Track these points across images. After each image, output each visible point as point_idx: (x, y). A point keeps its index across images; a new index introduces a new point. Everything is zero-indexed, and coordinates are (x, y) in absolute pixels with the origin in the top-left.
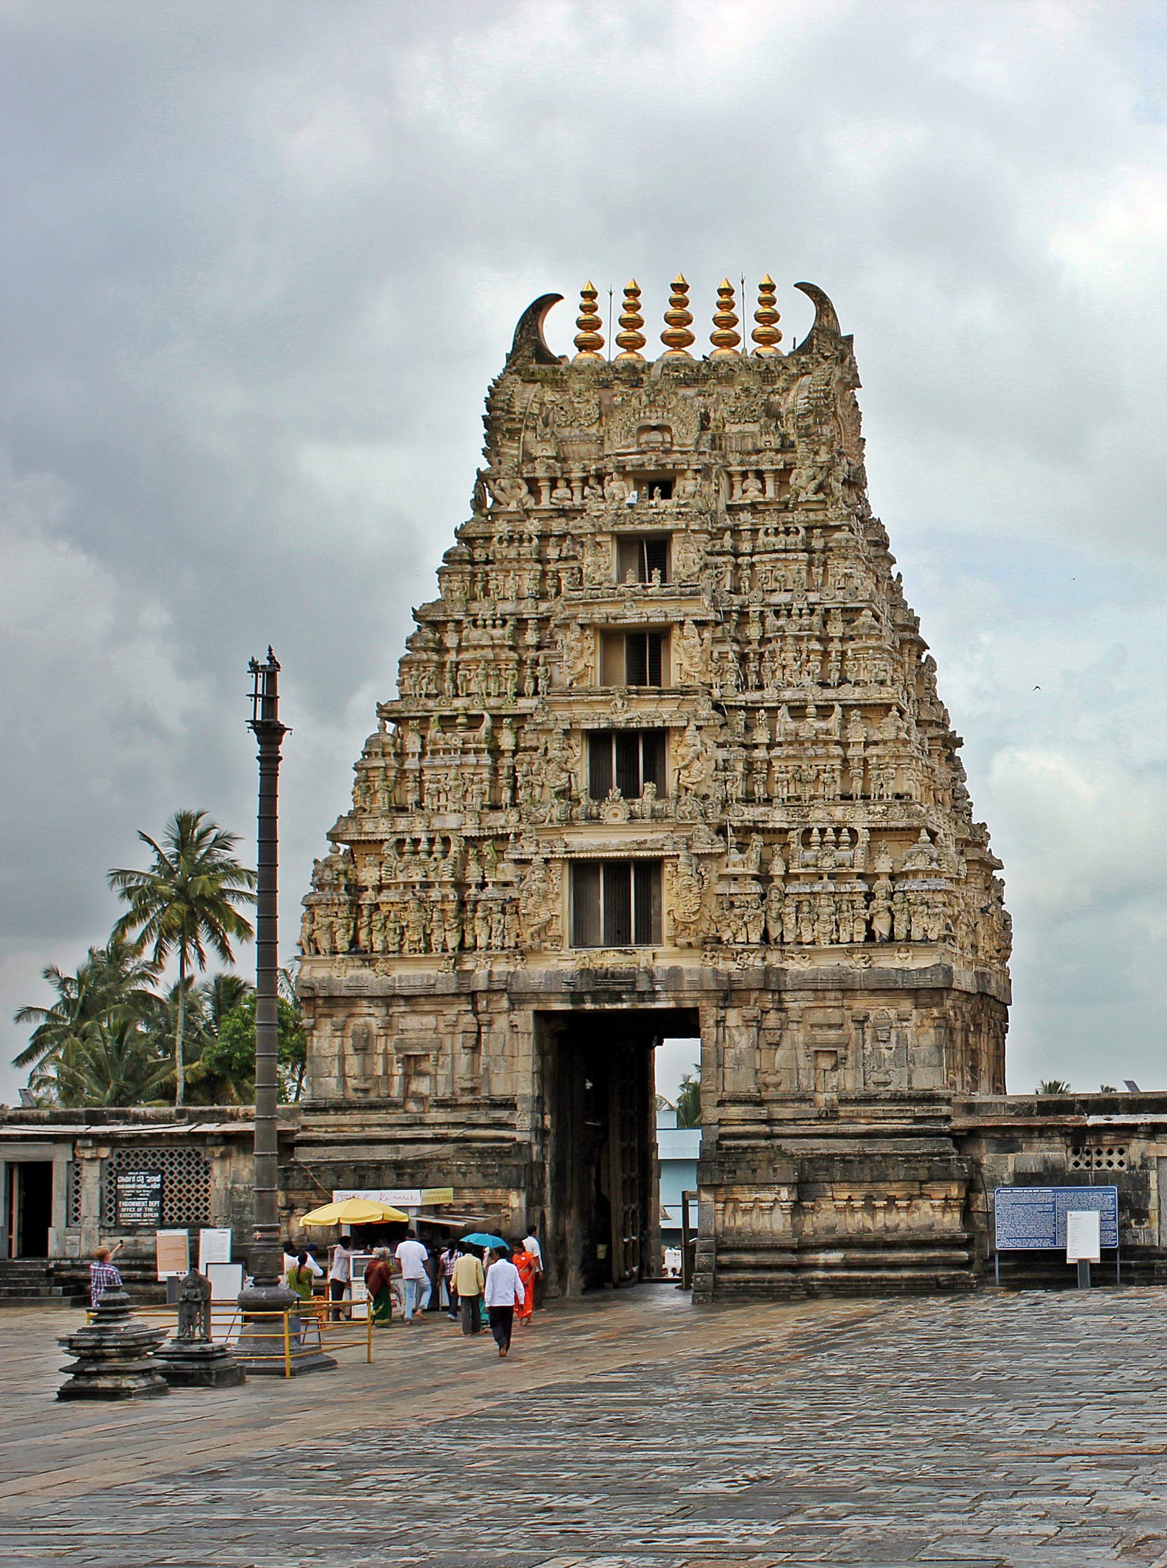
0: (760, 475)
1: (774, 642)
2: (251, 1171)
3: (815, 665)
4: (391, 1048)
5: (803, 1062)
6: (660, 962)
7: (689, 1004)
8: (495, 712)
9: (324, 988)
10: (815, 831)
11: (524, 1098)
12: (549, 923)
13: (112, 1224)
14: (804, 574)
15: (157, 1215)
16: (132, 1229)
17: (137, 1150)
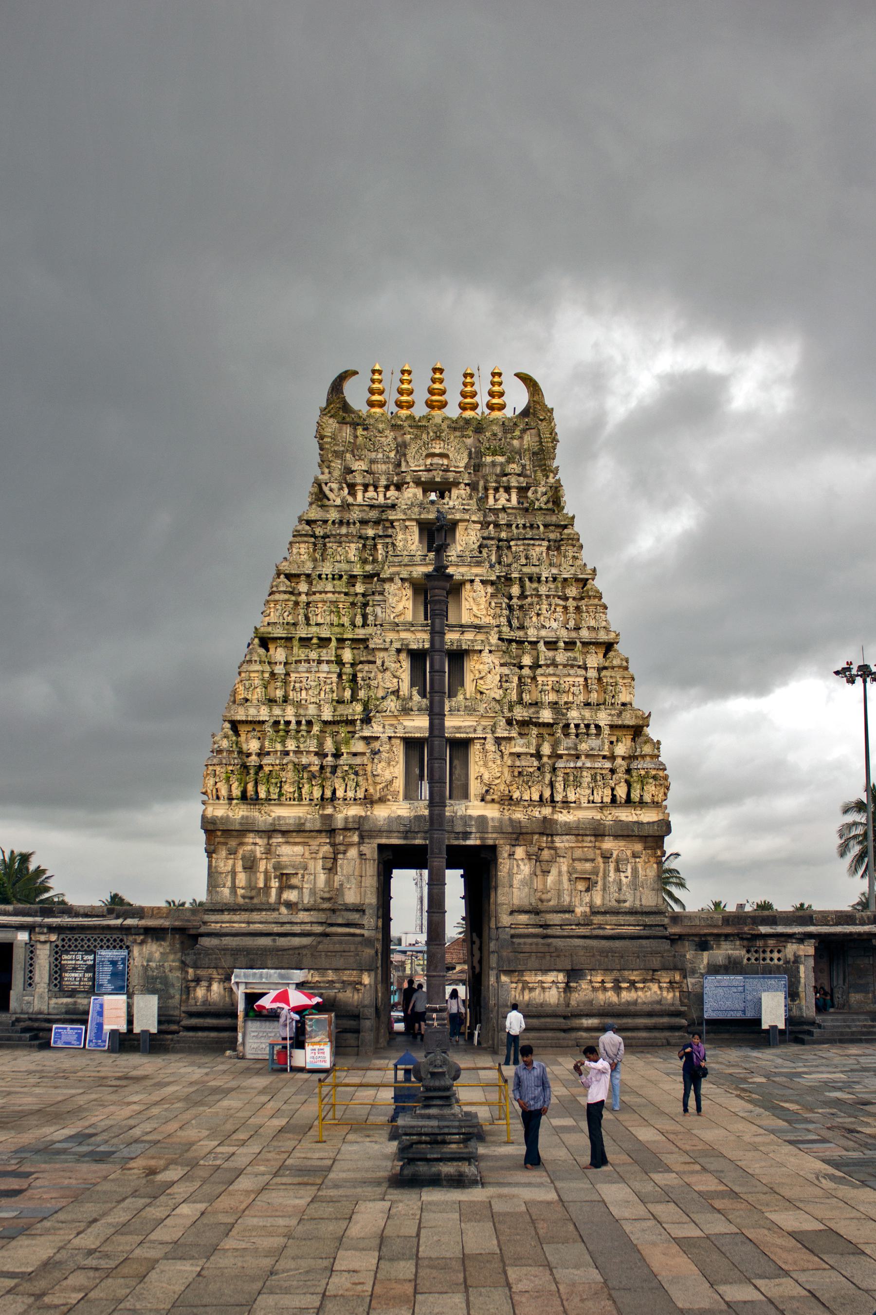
0: (507, 489)
1: (529, 598)
2: (161, 953)
3: (559, 615)
4: (270, 867)
5: (566, 884)
6: (469, 812)
7: (490, 842)
8: (339, 636)
9: (223, 824)
10: (572, 726)
11: (370, 904)
12: (391, 782)
13: (56, 989)
14: (544, 554)
15: (90, 983)
16: (73, 993)
17: (76, 936)
